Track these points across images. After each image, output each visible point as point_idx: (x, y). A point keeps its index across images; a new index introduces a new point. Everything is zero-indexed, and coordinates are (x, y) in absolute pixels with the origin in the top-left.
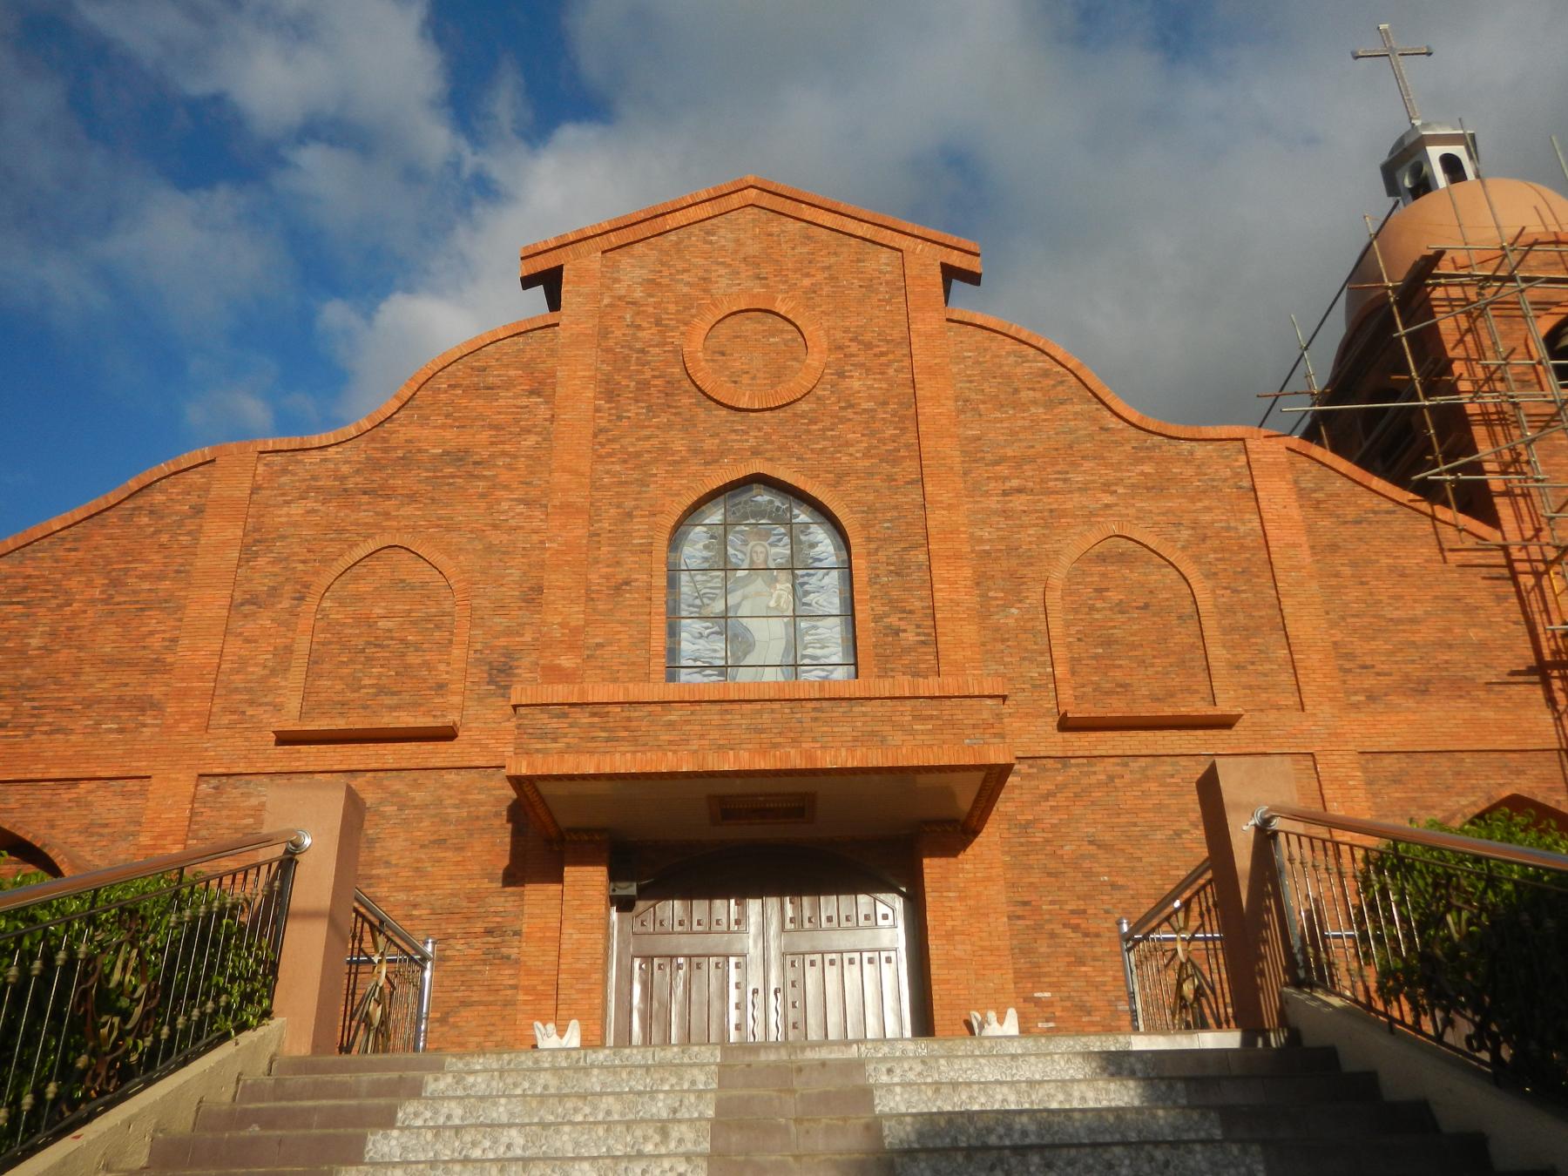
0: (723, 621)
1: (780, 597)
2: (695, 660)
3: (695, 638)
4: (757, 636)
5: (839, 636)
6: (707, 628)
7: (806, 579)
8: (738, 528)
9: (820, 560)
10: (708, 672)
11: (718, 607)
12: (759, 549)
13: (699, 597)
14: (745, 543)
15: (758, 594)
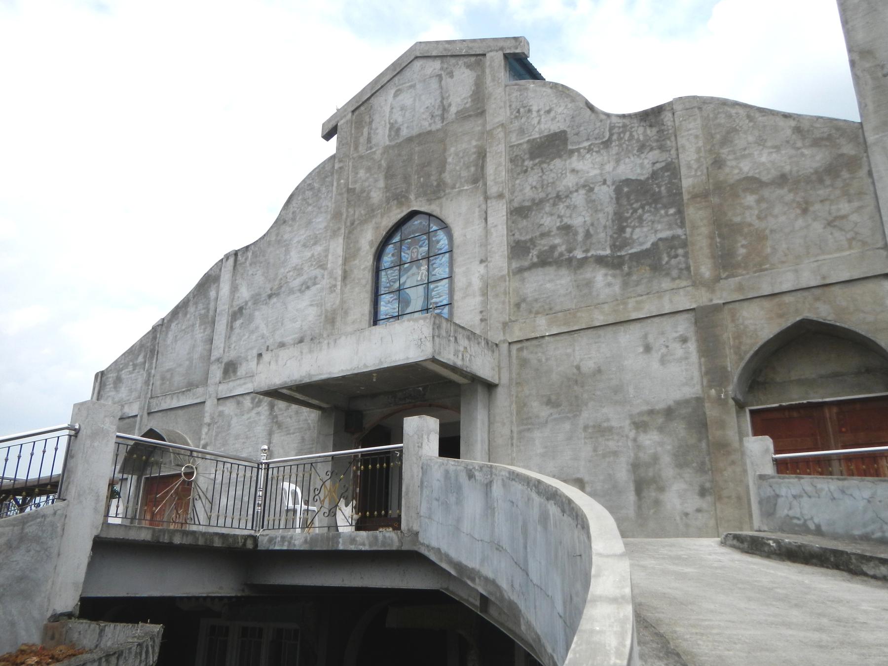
0: (398, 292)
1: (422, 274)
2: (386, 315)
3: (387, 304)
4: (412, 298)
5: (447, 289)
6: (391, 298)
7: (434, 261)
8: (406, 241)
9: (441, 249)
10: (391, 320)
11: (396, 285)
12: (415, 250)
13: (390, 282)
14: (409, 248)
15: (413, 275)
